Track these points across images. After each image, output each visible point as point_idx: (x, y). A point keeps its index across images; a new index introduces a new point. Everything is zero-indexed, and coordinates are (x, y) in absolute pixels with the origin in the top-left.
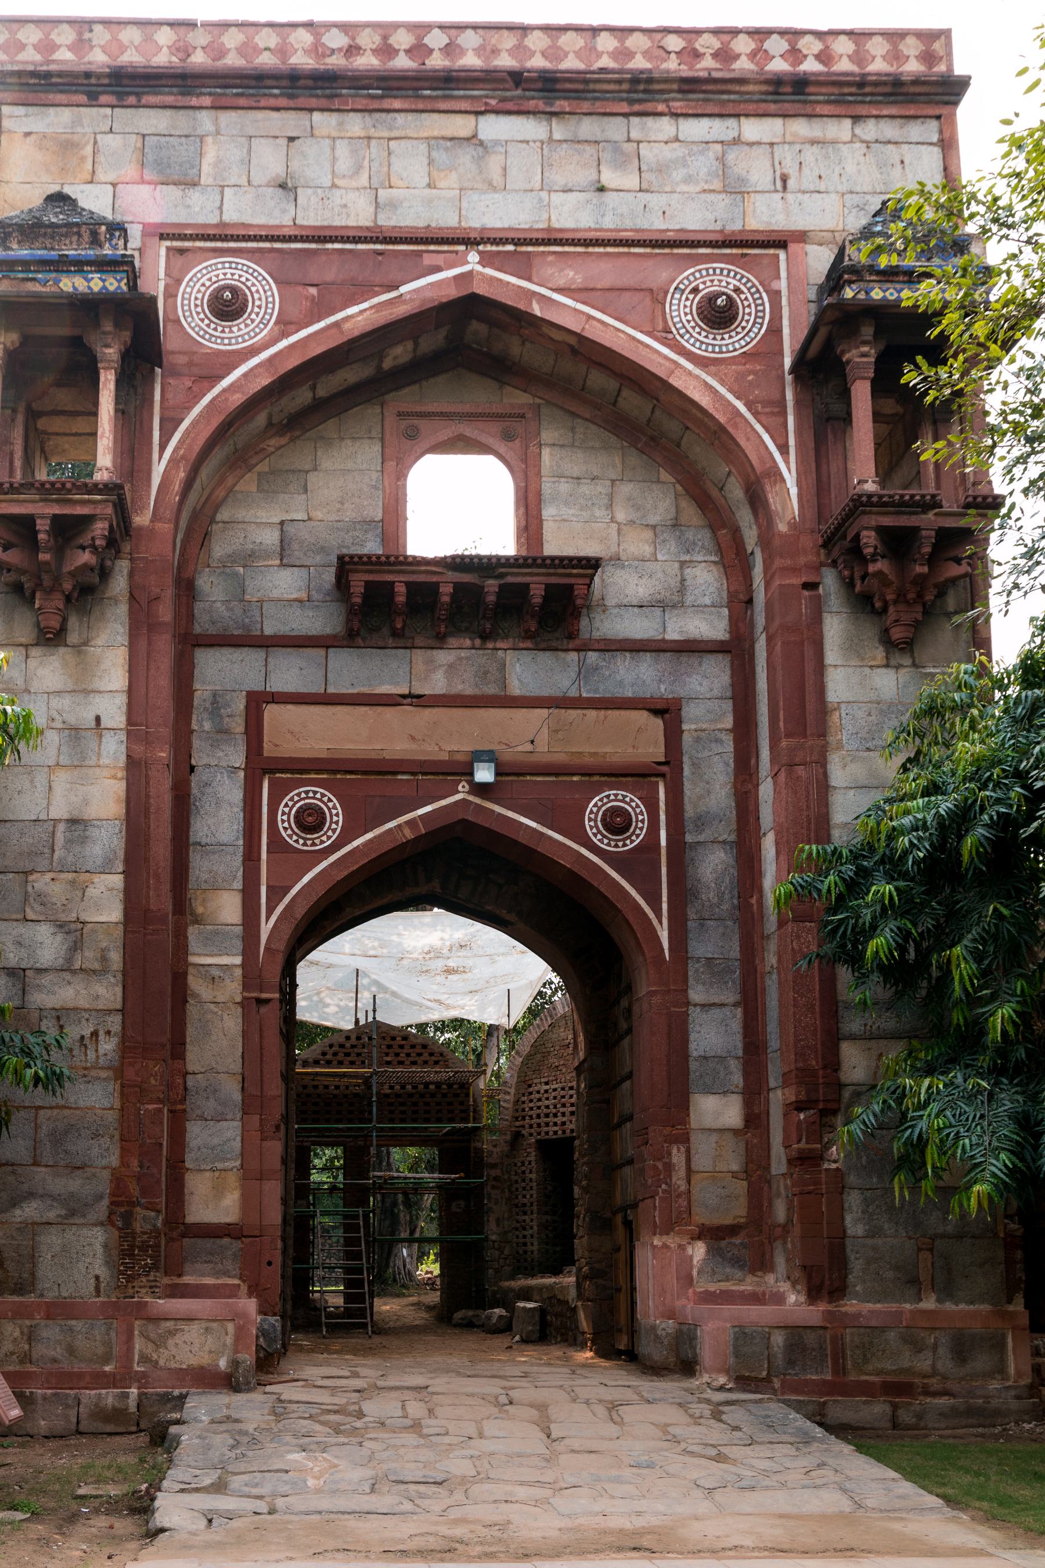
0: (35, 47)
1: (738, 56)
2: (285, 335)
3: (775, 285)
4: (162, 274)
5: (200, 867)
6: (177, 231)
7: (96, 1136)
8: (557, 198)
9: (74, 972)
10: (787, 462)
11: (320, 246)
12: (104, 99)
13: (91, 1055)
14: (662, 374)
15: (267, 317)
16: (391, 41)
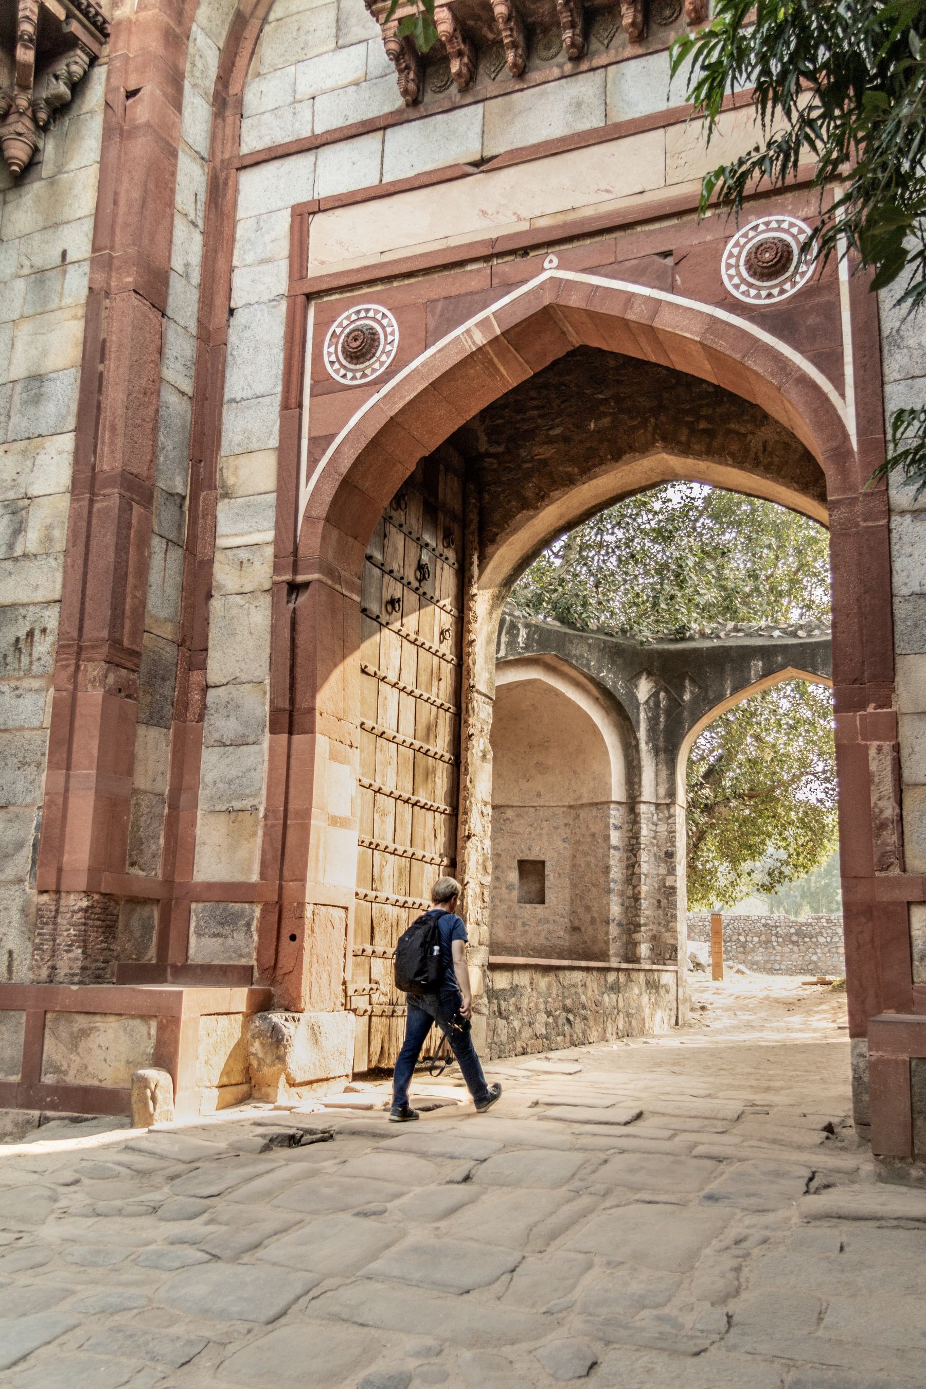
7: (24, 764)
9: (16, 559)
13: (25, 660)
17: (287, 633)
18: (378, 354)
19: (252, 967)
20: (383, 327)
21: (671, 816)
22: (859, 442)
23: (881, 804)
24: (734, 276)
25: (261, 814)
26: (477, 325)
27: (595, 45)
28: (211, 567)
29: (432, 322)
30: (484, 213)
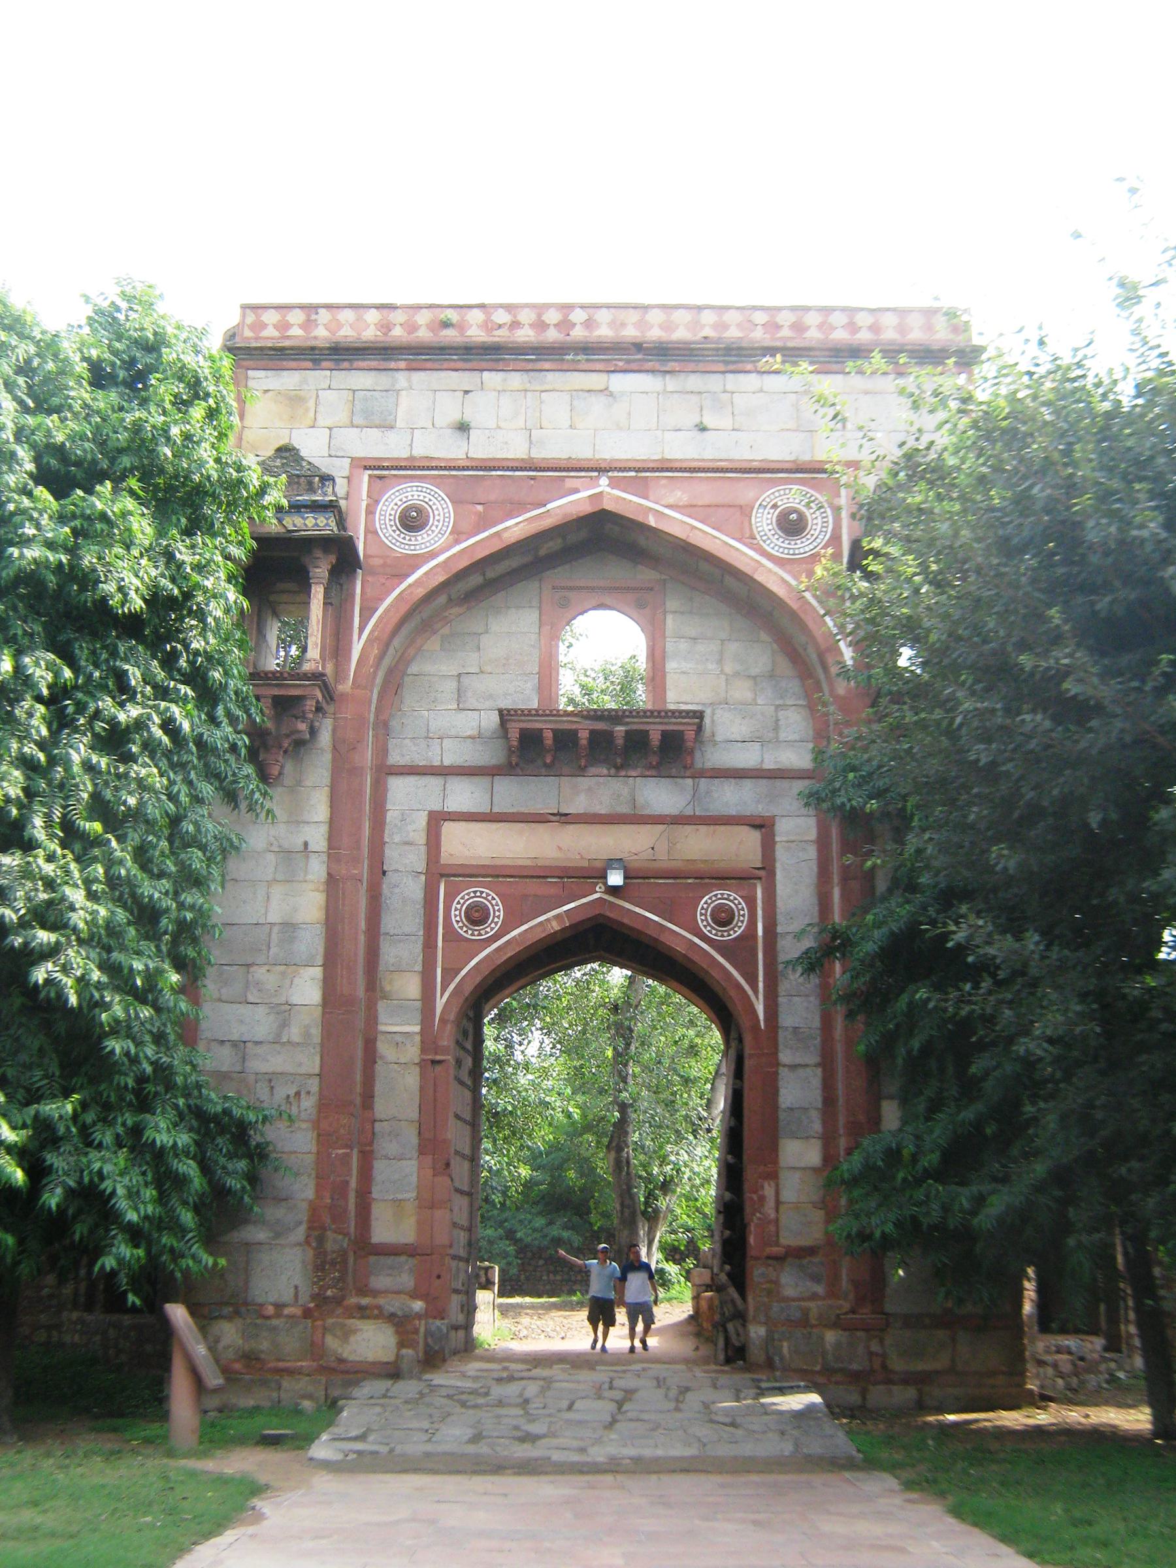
0: (275, 326)
1: (807, 328)
2: (457, 542)
3: (836, 501)
4: (364, 496)
5: (390, 953)
8: (669, 436)
12: (325, 364)
14: (749, 573)
16: (544, 318)
22: (766, 1026)
24: (703, 921)
30: (560, 848)
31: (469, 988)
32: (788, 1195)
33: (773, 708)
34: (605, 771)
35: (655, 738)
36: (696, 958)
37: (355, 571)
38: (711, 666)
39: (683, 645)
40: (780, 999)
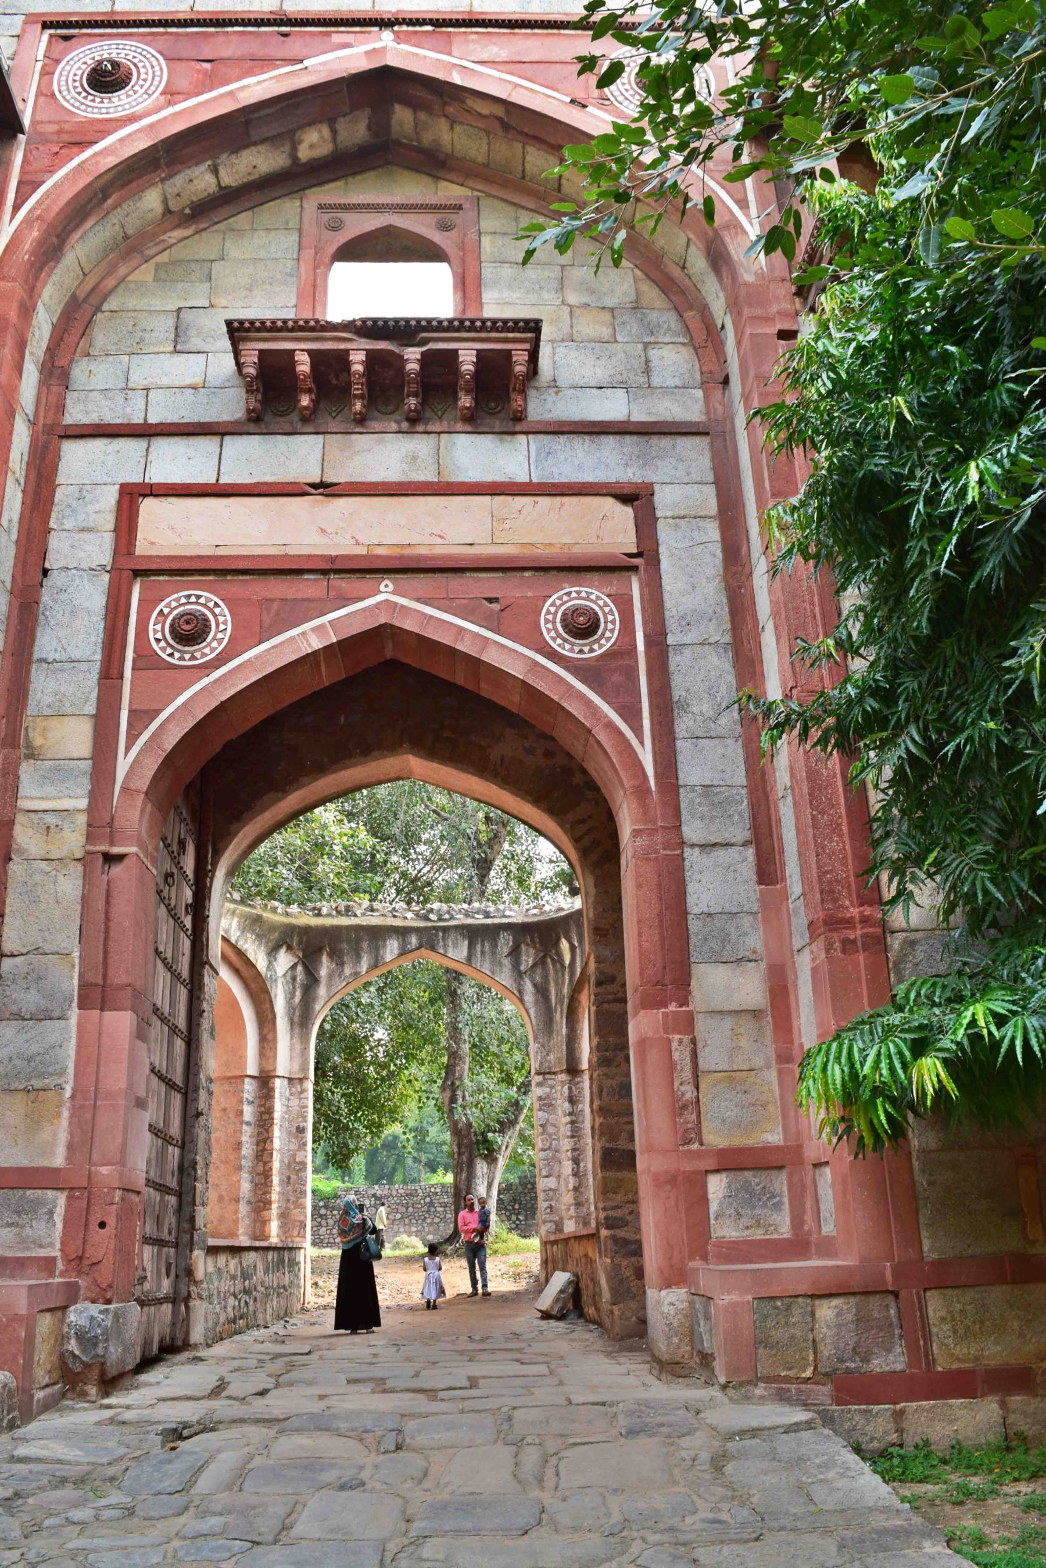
2: (170, 103)
4: (40, 56)
5: (43, 688)
6: (61, 19)
10: (748, 216)
11: (219, 29)
15: (153, 88)
17: (101, 905)
18: (209, 640)
19: (54, 1259)
20: (215, 615)
21: (303, 1091)
22: (656, 783)
23: (682, 1088)
24: (551, 632)
25: (68, 1093)
26: (313, 629)
27: (428, 414)
28: (11, 829)
29: (267, 620)
30: (323, 531)
31: (171, 741)
32: (711, 1058)
33: (640, 346)
34: (394, 426)
35: (467, 359)
36: (540, 685)
37: (15, 137)
38: (546, 296)
39: (507, 271)
40: (679, 744)
